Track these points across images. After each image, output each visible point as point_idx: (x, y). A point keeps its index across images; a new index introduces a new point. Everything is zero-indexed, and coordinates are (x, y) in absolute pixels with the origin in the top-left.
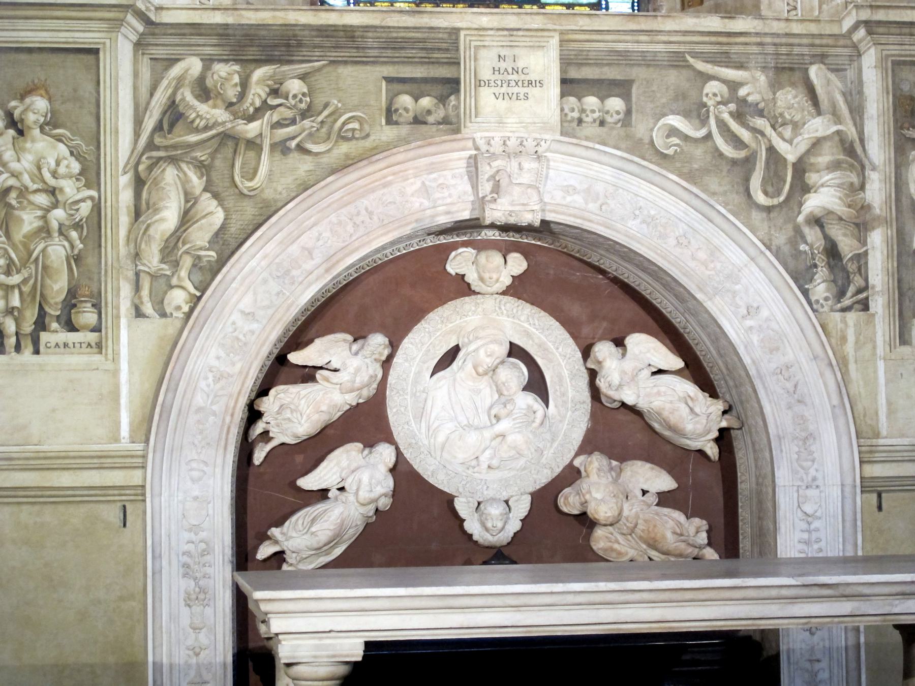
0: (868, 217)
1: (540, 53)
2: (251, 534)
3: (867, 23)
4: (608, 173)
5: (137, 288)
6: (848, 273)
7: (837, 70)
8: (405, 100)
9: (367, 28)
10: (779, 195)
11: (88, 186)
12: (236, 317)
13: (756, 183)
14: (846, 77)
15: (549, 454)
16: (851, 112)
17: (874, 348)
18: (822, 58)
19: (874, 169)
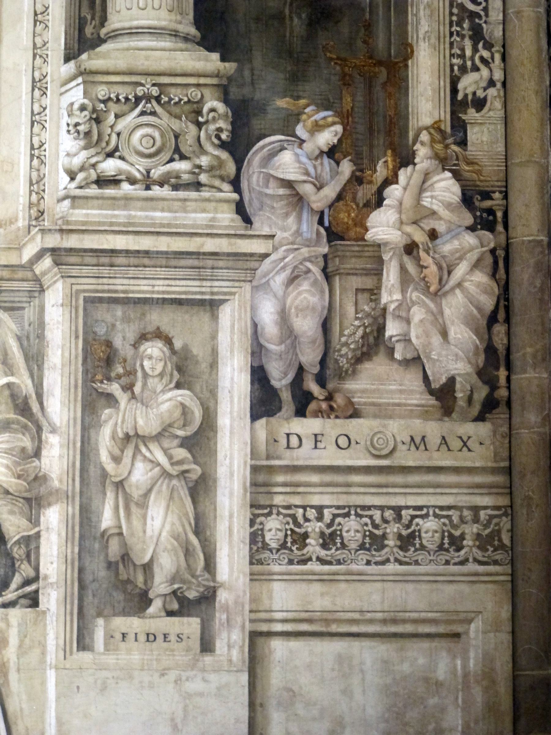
0: (43, 490)
3: (54, 251)
6: (13, 558)
14: (23, 317)
16: (27, 358)
17: (44, 653)
19: (53, 431)
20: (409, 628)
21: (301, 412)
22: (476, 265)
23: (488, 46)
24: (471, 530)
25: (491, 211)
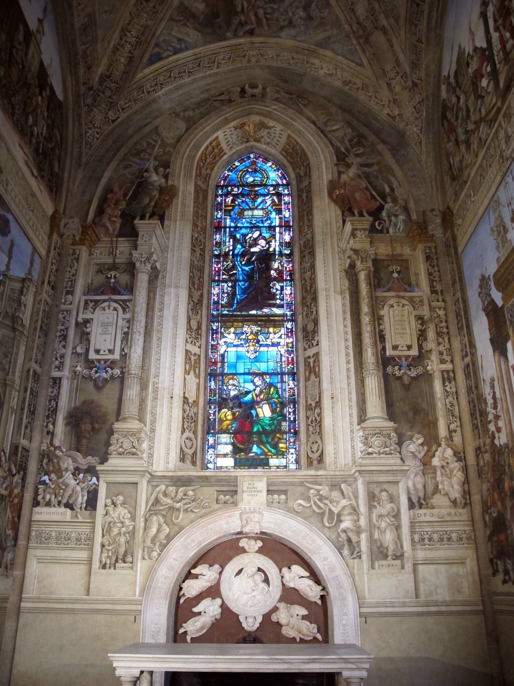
1: (261, 483)
2: (179, 625)
3: (359, 471)
4: (281, 517)
5: (144, 551)
7: (350, 485)
8: (222, 497)
9: (212, 476)
10: (332, 523)
11: (132, 521)
12: (171, 560)
13: (325, 520)
15: (269, 602)
18: (345, 482)
19: (362, 515)
20: (452, 561)
21: (420, 508)
22: (459, 470)
23: (456, 417)
24: (464, 536)
25: (461, 457)
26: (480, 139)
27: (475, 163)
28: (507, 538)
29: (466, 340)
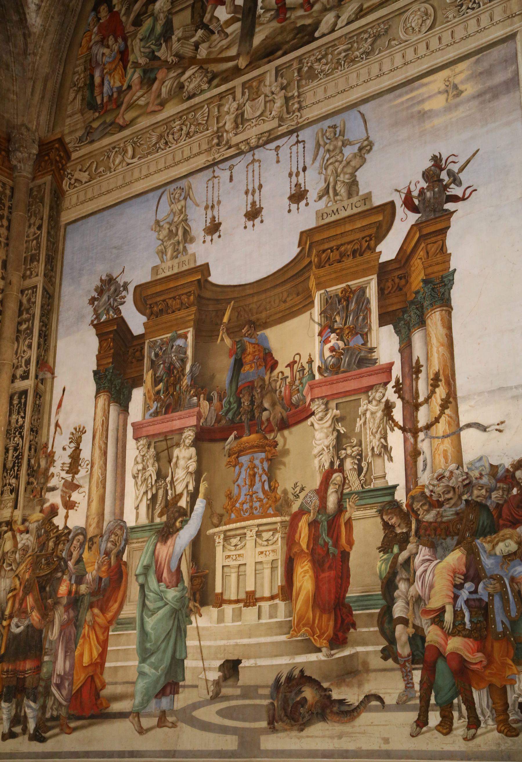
26: (181, 87)
27: (154, 112)
28: (38, 669)
29: (33, 354)
